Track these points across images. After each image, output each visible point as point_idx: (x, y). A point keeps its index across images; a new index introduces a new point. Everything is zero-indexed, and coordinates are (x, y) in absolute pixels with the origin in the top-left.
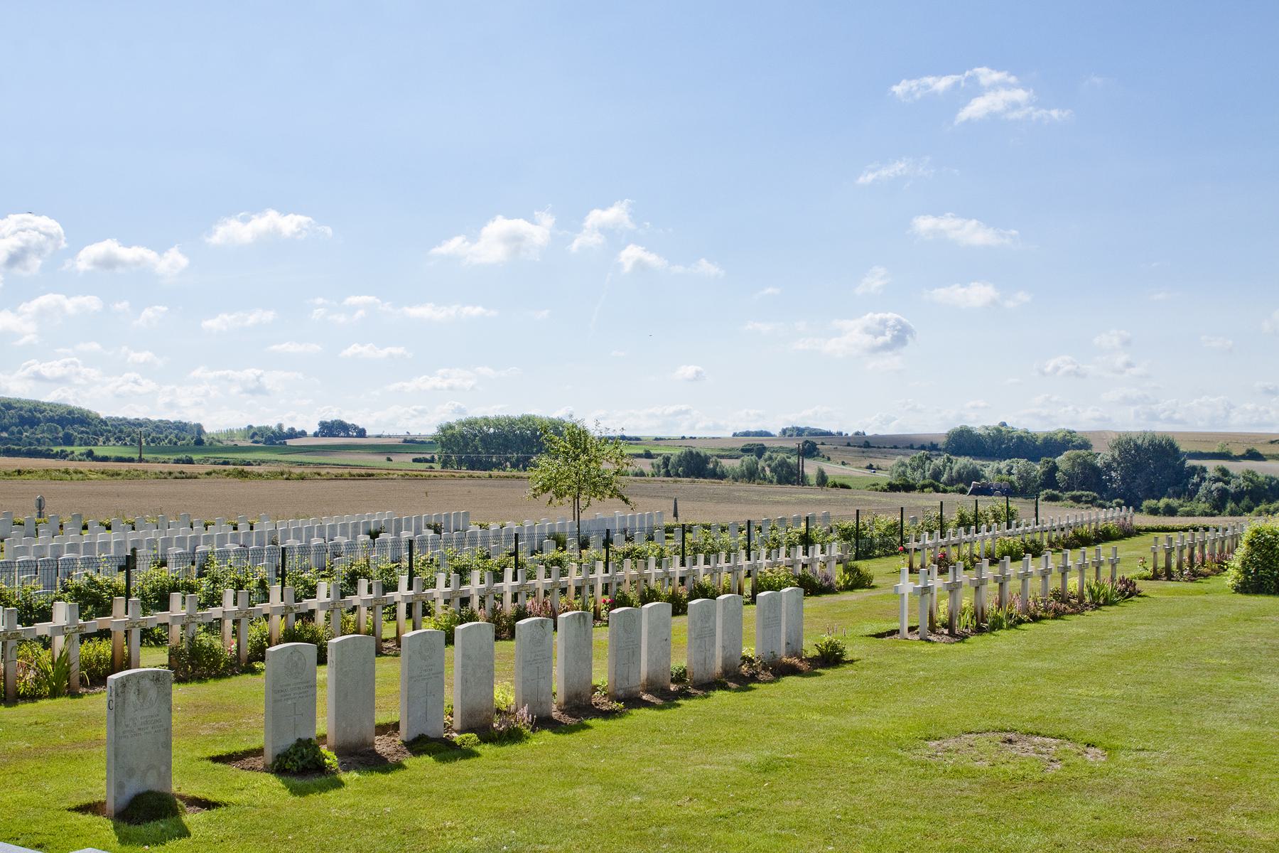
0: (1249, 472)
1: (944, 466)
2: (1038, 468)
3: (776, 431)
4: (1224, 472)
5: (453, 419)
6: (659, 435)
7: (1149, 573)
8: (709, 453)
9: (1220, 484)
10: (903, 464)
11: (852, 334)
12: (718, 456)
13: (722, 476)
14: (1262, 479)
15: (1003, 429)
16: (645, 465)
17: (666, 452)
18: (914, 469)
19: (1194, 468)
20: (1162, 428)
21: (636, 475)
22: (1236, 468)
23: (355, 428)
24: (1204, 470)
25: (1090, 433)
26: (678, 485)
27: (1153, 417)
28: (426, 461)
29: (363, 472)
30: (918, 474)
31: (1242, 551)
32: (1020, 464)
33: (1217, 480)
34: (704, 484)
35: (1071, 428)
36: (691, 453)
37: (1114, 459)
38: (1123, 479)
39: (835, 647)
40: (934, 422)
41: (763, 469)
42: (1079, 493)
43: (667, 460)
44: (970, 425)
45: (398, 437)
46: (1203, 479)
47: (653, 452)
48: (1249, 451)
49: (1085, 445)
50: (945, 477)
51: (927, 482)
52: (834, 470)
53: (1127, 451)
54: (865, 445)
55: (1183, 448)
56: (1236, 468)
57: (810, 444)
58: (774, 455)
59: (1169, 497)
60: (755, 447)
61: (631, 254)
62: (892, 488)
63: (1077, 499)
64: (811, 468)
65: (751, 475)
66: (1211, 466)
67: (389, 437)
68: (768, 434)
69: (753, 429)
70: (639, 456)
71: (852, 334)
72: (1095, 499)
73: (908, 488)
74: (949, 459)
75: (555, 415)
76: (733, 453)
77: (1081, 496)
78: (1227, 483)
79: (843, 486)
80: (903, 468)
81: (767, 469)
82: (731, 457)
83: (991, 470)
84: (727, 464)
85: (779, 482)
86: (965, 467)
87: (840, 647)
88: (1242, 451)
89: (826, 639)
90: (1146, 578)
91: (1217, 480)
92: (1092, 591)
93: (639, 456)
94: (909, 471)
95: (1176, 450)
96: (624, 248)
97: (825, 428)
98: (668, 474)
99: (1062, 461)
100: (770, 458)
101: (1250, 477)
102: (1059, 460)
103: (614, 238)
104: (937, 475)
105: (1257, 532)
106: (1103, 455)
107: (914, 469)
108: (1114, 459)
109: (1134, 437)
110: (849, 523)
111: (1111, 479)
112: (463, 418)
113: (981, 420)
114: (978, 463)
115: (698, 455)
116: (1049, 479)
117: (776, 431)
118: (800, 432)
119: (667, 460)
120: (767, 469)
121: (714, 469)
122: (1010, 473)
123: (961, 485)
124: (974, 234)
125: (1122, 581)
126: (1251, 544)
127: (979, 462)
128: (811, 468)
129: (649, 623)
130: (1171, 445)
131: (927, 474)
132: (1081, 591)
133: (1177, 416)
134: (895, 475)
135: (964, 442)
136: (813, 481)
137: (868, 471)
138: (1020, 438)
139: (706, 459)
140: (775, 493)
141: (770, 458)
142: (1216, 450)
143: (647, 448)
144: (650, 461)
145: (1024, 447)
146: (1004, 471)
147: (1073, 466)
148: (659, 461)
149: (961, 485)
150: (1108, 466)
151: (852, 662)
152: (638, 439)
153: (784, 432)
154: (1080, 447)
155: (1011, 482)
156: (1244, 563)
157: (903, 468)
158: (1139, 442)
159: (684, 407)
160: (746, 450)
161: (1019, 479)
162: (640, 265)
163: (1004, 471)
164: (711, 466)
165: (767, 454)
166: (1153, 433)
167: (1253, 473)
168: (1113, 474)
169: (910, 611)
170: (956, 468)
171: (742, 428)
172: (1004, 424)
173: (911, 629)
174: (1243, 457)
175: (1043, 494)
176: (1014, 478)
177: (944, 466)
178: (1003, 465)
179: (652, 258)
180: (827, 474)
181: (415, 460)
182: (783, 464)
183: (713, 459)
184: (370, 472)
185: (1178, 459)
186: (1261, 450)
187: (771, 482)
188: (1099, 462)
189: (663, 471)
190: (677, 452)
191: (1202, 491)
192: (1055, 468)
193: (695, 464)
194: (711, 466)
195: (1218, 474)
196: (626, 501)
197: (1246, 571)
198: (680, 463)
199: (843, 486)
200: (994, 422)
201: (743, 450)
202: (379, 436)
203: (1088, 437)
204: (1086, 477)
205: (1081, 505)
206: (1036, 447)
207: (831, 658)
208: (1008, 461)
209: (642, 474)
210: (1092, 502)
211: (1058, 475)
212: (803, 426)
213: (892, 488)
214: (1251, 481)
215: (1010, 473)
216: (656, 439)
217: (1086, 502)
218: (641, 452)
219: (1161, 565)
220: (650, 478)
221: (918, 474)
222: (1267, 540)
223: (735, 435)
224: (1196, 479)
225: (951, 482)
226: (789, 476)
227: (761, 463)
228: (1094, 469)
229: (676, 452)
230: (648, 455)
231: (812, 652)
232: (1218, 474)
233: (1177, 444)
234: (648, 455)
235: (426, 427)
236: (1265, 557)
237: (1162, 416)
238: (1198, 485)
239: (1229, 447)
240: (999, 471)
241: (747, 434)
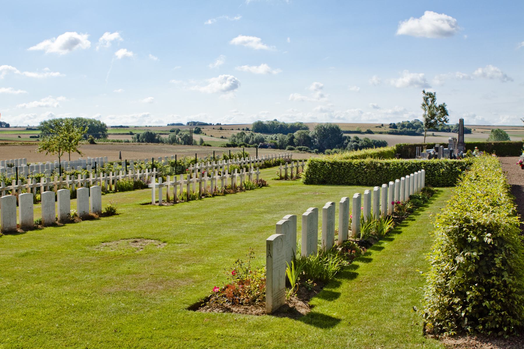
0: (366, 138)
1: (250, 137)
2: (287, 137)
3: (185, 123)
4: (357, 138)
5: (47, 120)
6: (136, 125)
7: (278, 177)
8: (156, 132)
9: (355, 143)
10: (234, 136)
11: (216, 84)
12: (161, 134)
13: (162, 142)
14: (371, 141)
15: (275, 122)
16: (130, 138)
17: (138, 132)
18: (238, 138)
19: (346, 137)
20: (334, 121)
21: (126, 142)
22: (361, 137)
23: (5, 123)
24: (350, 138)
25: (309, 123)
26: (140, 146)
27: (332, 117)
28: (36, 137)
29: (3, 142)
30: (240, 140)
31: (306, 168)
32: (280, 136)
33: (354, 141)
34: (151, 145)
35: (301, 121)
36: (148, 132)
37: (316, 134)
38: (319, 142)
39: (112, 209)
40: (249, 119)
41: (178, 139)
42: (301, 147)
43: (138, 136)
44: (262, 121)
45: (24, 127)
46: (349, 141)
47: (133, 132)
48: (368, 130)
49: (306, 128)
50: (250, 142)
51: (242, 143)
52: (207, 139)
53: (320, 131)
54: (221, 128)
55: (342, 129)
56: (361, 137)
57: (198, 127)
58: (183, 133)
59: (336, 148)
60: (175, 129)
61: (121, 53)
62: (228, 146)
63: (300, 150)
64: (196, 138)
65: (173, 141)
66: (352, 136)
67: (20, 127)
68: (181, 125)
69: (175, 122)
70: (127, 134)
71: (216, 84)
72: (307, 149)
73: (234, 146)
74: (252, 134)
75: (91, 118)
76: (166, 132)
77: (302, 148)
78: (358, 143)
79: (208, 145)
80: (234, 138)
81: (180, 139)
82: (166, 134)
83: (269, 138)
84: (163, 136)
85: (185, 144)
86: (259, 137)
87: (114, 208)
88: (365, 130)
89: (109, 205)
90: (277, 179)
91: (354, 141)
92: (245, 185)
93: (127, 134)
94: (236, 139)
95: (339, 130)
96: (119, 49)
97: (205, 122)
98: (139, 141)
99: (296, 134)
100: (181, 134)
101: (366, 140)
102: (295, 134)
103: (115, 45)
104: (247, 141)
105: (312, 161)
106: (312, 132)
107: (238, 138)
108: (316, 134)
109: (323, 125)
110: (173, 160)
111: (315, 141)
112: (51, 119)
113: (266, 118)
114: (263, 135)
115: (151, 133)
116: (291, 142)
117: (185, 123)
118: (194, 123)
119: (138, 136)
120: (180, 139)
121: (158, 139)
122: (276, 139)
123: (256, 144)
124: (255, 42)
125: (261, 180)
126: (309, 165)
127: (265, 135)
128: (196, 138)
129: (21, 201)
130: (337, 128)
131: (244, 140)
132: (241, 184)
133: (342, 117)
134: (231, 141)
135: (260, 127)
136: (199, 143)
137: (221, 139)
138: (281, 126)
139: (155, 135)
140: (180, 148)
141: (181, 134)
142: (356, 130)
143: (131, 130)
144: (131, 136)
145: (283, 129)
146: (274, 139)
147: (300, 136)
148: (135, 136)
149: (256, 144)
150: (314, 136)
151: (118, 214)
152: (127, 127)
153: (188, 123)
154: (303, 129)
155: (275, 143)
156: (306, 173)
157: (234, 138)
158: (325, 127)
159: (147, 113)
160: (172, 131)
161: (280, 141)
162: (125, 57)
163: (274, 139)
164: (157, 138)
165: (180, 133)
166: (331, 124)
167: (368, 139)
168: (315, 139)
169: (156, 196)
170: (255, 137)
171: (171, 122)
172: (276, 120)
173: (157, 202)
174: (366, 133)
175: (287, 147)
176: (277, 141)
177: (250, 137)
178: (274, 136)
179: (130, 54)
180: (204, 141)
181: (31, 137)
182: (186, 136)
183: (158, 135)
184: (6, 142)
185: (340, 133)
186: (372, 130)
187: (181, 144)
188: (310, 135)
189: (137, 140)
190: (143, 132)
191: (349, 146)
192: (293, 137)
193: (150, 137)
194: (157, 138)
195: (355, 139)
196: (79, 153)
197: (307, 176)
198: (144, 137)
199: (208, 145)
200: (272, 119)
201: (171, 131)
202: (16, 127)
203: (308, 125)
204: (305, 141)
205: (302, 152)
206: (287, 129)
207: (111, 213)
208: (275, 135)
209: (128, 142)
210: (306, 150)
211: (295, 140)
212: (196, 121)
213: (228, 146)
214: (367, 142)
215: (276, 139)
216: (135, 127)
217: (304, 150)
218: (129, 132)
219: (289, 175)
220: (123, 143)
221: (240, 140)
222: (315, 164)
223: (168, 125)
224: (346, 141)
225: (253, 143)
226: (188, 141)
227: (177, 136)
228: (308, 137)
229: (142, 133)
230: (131, 134)
231: (104, 210)
232: (355, 139)
233: (340, 128)
234: (131, 134)
235: (36, 123)
236: (314, 170)
237: (336, 117)
238: (347, 143)
239: (361, 129)
240: (272, 139)
241: (173, 125)
